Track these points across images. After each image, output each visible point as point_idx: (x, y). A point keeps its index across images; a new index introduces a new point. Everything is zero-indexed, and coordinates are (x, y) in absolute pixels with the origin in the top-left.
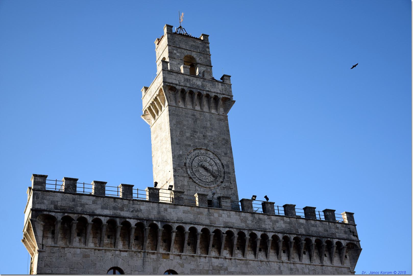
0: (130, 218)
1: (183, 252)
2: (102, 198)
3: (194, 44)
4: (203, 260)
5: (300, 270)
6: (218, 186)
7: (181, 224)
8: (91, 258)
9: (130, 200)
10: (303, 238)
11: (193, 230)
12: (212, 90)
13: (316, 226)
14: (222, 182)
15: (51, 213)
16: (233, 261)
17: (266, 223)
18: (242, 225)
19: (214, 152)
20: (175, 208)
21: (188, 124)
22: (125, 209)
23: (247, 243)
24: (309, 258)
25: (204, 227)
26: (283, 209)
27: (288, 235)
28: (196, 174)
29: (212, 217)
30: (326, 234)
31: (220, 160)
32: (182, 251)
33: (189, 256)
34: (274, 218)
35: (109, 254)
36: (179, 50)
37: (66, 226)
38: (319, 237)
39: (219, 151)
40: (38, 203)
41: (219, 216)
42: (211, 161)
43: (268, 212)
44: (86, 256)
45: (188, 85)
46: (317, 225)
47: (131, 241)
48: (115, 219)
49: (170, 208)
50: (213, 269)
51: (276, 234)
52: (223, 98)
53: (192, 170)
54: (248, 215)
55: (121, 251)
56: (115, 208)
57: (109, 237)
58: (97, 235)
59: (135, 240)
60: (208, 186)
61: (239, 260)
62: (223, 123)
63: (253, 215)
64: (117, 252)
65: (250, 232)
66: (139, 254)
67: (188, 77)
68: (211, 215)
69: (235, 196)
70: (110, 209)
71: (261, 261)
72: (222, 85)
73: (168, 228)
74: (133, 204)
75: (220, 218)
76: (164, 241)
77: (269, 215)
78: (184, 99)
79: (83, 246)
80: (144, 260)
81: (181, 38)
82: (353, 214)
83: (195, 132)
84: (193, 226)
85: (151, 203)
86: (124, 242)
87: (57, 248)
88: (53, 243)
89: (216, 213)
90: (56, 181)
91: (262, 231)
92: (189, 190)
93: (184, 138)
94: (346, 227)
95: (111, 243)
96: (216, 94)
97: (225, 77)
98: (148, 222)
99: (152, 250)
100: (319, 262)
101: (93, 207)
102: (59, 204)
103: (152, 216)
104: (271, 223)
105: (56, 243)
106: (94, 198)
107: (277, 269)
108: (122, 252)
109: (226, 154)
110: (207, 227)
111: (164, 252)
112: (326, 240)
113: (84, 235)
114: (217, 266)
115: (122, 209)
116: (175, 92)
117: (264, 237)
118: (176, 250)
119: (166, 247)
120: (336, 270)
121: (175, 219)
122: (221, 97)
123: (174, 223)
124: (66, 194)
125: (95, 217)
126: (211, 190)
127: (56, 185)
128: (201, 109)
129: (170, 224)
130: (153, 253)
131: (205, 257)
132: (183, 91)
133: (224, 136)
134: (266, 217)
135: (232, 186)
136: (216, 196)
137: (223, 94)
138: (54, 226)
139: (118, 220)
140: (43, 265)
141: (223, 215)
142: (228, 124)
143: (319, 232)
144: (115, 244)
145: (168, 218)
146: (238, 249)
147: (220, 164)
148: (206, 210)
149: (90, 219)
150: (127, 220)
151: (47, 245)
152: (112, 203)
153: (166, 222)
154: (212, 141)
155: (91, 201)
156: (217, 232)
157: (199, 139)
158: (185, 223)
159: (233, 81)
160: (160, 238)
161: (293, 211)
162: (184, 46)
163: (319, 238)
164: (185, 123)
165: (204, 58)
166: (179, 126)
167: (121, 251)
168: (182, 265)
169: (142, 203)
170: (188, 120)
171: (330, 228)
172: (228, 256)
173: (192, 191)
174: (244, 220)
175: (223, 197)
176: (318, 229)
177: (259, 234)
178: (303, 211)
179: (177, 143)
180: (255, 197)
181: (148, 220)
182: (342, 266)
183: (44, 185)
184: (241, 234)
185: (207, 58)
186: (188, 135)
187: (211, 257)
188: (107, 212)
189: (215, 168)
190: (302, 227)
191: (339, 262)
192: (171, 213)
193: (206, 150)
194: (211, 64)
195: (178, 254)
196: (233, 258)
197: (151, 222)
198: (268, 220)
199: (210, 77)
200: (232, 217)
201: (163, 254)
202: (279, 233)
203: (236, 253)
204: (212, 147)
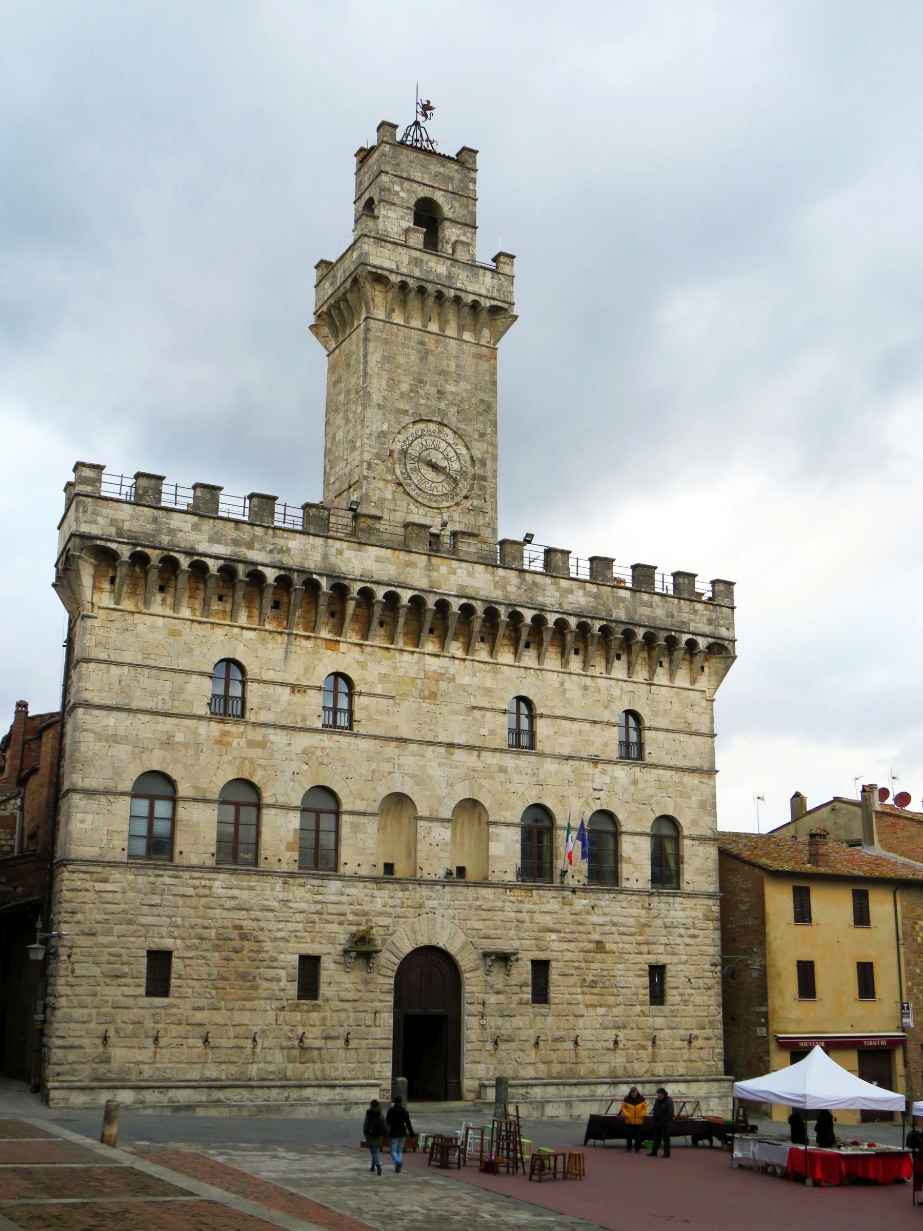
0: (266, 565)
1: (366, 640)
2: (212, 521)
3: (442, 170)
4: (406, 657)
5: (603, 691)
6: (457, 504)
7: (368, 585)
8: (183, 638)
9: (267, 528)
10: (621, 628)
11: (392, 599)
12: (469, 288)
13: (651, 606)
14: (466, 497)
15: (109, 545)
16: (467, 662)
17: (547, 593)
18: (496, 594)
19: (458, 428)
20: (359, 550)
21: (408, 363)
22: (256, 546)
23: (502, 630)
24: (626, 667)
25: (416, 593)
26: (588, 564)
27: (589, 621)
28: (413, 476)
29: (435, 574)
30: (668, 623)
31: (468, 449)
32: (365, 637)
33: (380, 647)
34: (564, 583)
35: (219, 632)
36: (407, 185)
37: (138, 569)
38: (654, 628)
39: (469, 429)
40: (85, 522)
41: (450, 573)
42: (449, 449)
43: (555, 570)
44: (174, 633)
45: (417, 273)
46: (654, 604)
47: (264, 611)
48: (233, 564)
49: (349, 549)
50: (425, 678)
51: (565, 617)
52: (492, 306)
53: (406, 468)
54: (512, 575)
55: (242, 628)
56: (236, 543)
57: (220, 598)
58: (198, 592)
59: (272, 607)
60: (434, 505)
61: (480, 662)
62: (484, 366)
63: (522, 574)
64: (236, 630)
65: (510, 610)
66: (278, 637)
67: (418, 254)
68: (433, 570)
69: (490, 530)
70: (226, 545)
71: (526, 668)
72: (493, 278)
73: (340, 590)
74: (274, 536)
75: (452, 577)
76: (332, 615)
77: (556, 577)
78: (404, 304)
79: (169, 612)
80: (287, 649)
81: (412, 155)
82: (733, 584)
83: (421, 381)
84: (392, 589)
85: (311, 537)
86: (250, 612)
87: (120, 613)
88: (112, 602)
89: (443, 567)
90: (122, 476)
91: (535, 609)
92: (395, 510)
93: (396, 395)
94: (713, 611)
95: (224, 612)
96: (477, 298)
97: (502, 259)
98: (301, 575)
99: (306, 630)
100: (647, 676)
101: (193, 537)
102: (127, 526)
103: (310, 565)
104: (557, 594)
105: (117, 602)
106: (196, 519)
107: (557, 684)
108: (245, 631)
109: (482, 435)
110: (421, 594)
111: (329, 636)
112: (666, 634)
113: (172, 590)
114: (434, 672)
115: (250, 546)
116: (386, 286)
117: (539, 621)
118: (354, 634)
119: (333, 626)
120: (677, 694)
121: (358, 573)
122: (488, 304)
123: (355, 580)
124: (140, 508)
125: (196, 558)
126: (441, 513)
127: (121, 485)
128: (440, 328)
129: (346, 582)
130: (308, 638)
131: (413, 652)
132: (403, 286)
133: (482, 396)
134: (548, 580)
135: (488, 507)
136: (450, 528)
137: (494, 299)
138: (115, 568)
139: (241, 568)
140: (93, 644)
141: (459, 571)
142: (495, 368)
143: (654, 619)
144: (233, 615)
145: (344, 569)
146: (482, 640)
147: (468, 458)
148: (425, 557)
149: (185, 562)
150: (260, 568)
151: (102, 605)
152: (230, 531)
153: (339, 577)
154: (455, 405)
155: (190, 525)
156: (442, 606)
157: (428, 399)
158: (378, 583)
159: (518, 268)
160: (322, 609)
161: (608, 572)
162: (417, 176)
163: (652, 630)
164: (401, 360)
165: (462, 205)
166: (387, 367)
167: (242, 628)
168: (363, 665)
169: (291, 535)
170: (409, 354)
171: (680, 610)
172: (460, 653)
173: (399, 514)
174: (502, 585)
175: (464, 533)
176: (653, 611)
177: (528, 615)
178: (630, 572)
179: (379, 405)
180: (532, 536)
181: (301, 571)
182: (691, 687)
183: (98, 485)
184: (491, 613)
185: (467, 206)
186: (405, 387)
187: (424, 654)
188: (219, 549)
189: (456, 465)
190: (622, 605)
191: (688, 679)
192: (349, 559)
193: (441, 424)
194: (475, 221)
195: (357, 641)
196: (469, 657)
197: (306, 576)
198: (553, 587)
199: (468, 257)
200: (476, 575)
201: (326, 640)
202: (571, 614)
203: (477, 647)
204: (454, 419)
